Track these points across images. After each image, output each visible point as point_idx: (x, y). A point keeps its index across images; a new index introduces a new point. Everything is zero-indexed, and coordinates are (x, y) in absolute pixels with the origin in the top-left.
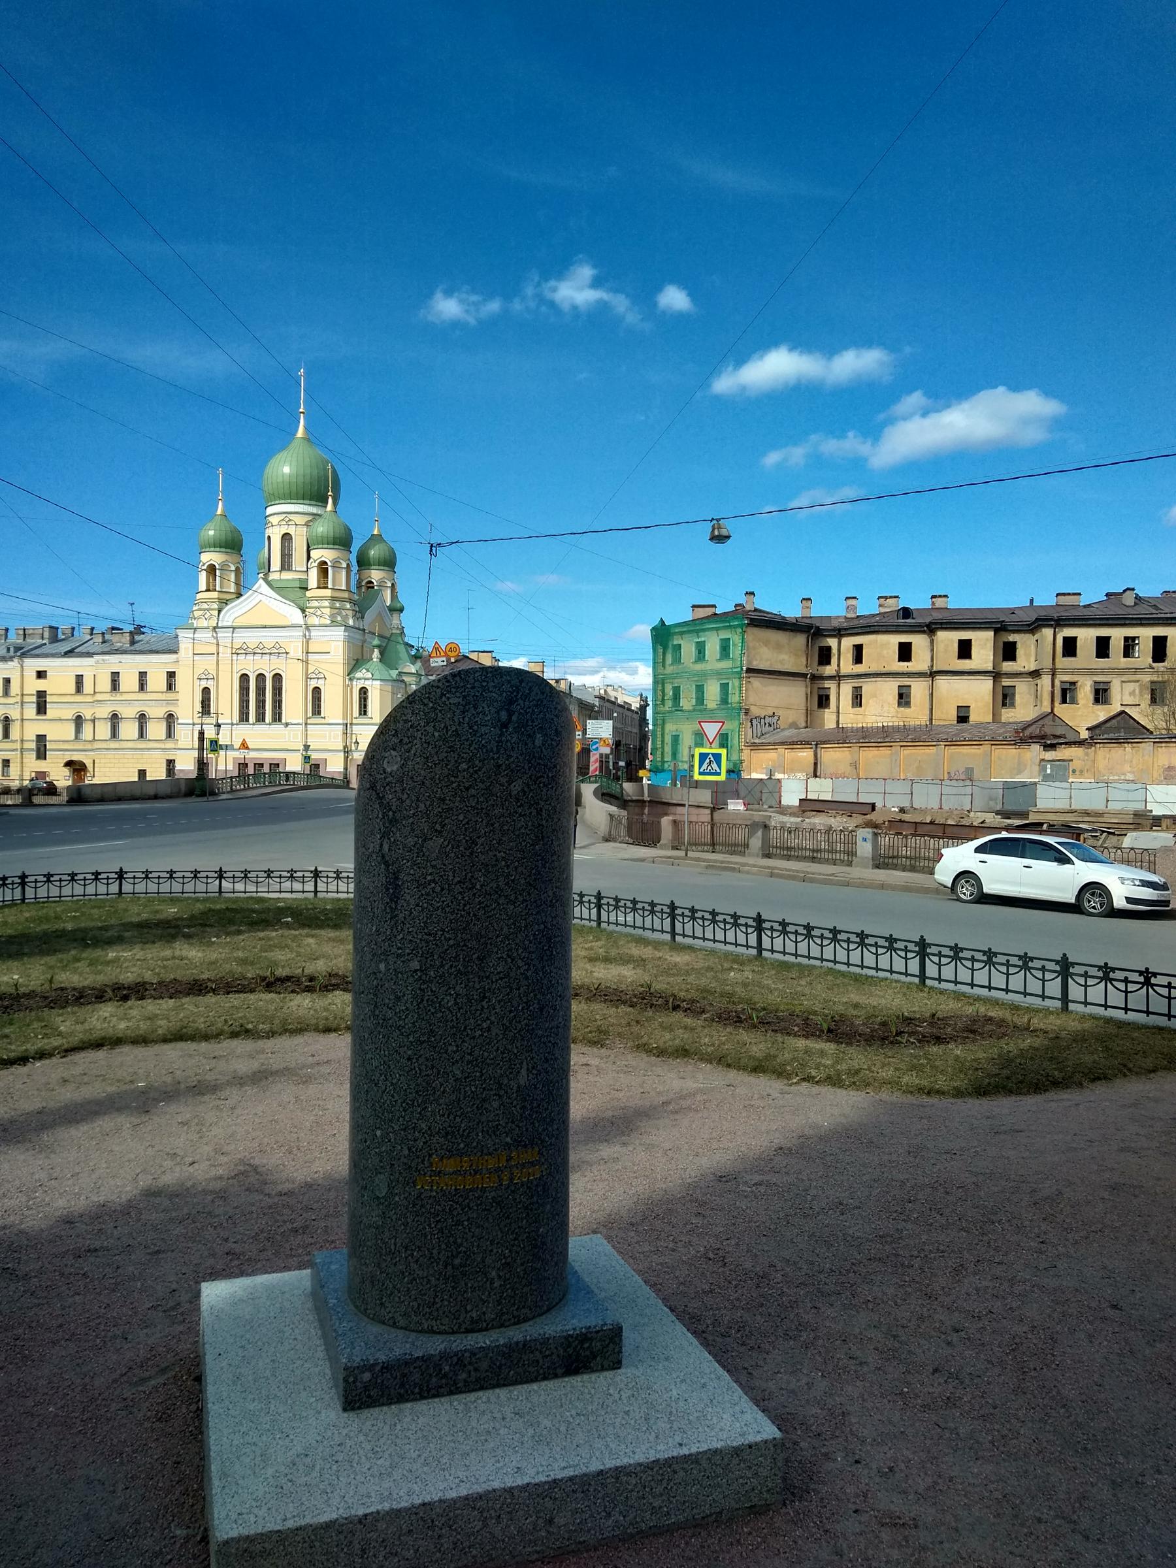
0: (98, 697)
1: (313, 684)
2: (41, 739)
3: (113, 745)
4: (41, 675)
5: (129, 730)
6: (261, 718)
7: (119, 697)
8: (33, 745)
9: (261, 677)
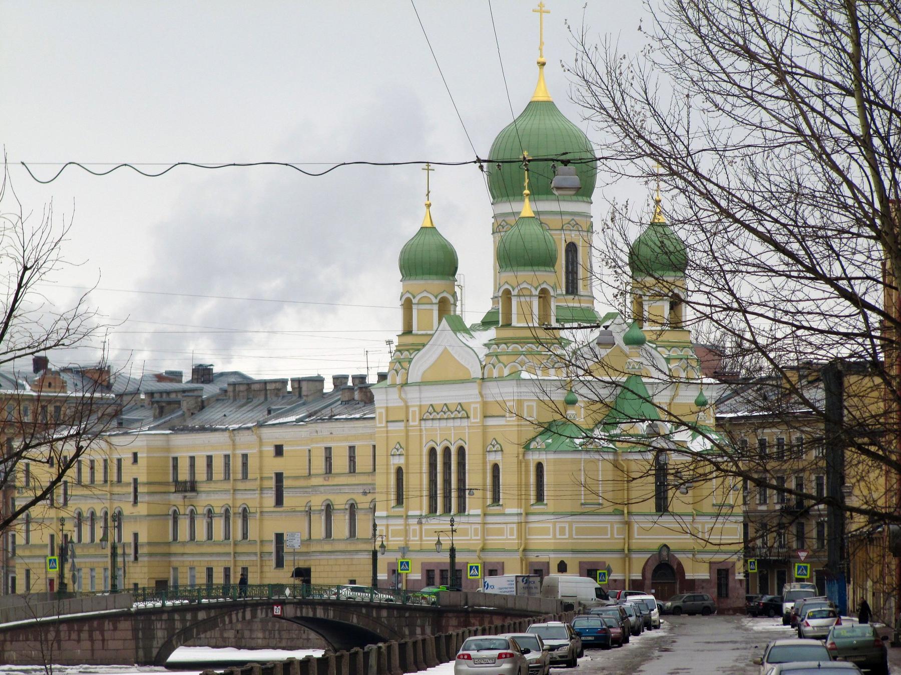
0: (315, 481)
1: (492, 458)
2: (279, 537)
4: (279, 451)
8: (272, 548)
9: (447, 451)
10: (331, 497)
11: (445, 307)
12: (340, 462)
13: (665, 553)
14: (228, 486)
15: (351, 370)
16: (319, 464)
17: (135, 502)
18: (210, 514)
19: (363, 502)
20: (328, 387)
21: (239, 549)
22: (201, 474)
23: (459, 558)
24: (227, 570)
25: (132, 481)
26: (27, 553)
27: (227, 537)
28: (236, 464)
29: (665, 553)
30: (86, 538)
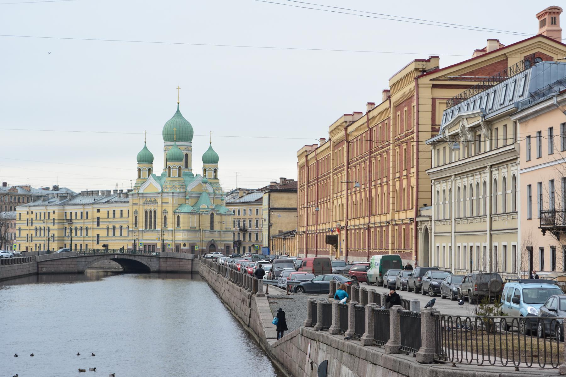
2: (98, 236)
3: (114, 239)
4: (98, 211)
5: (118, 232)
6: (151, 228)
7: (115, 220)
8: (96, 239)
9: (151, 212)
10: (115, 224)
11: (150, 170)
12: (118, 214)
13: (213, 241)
14: (82, 221)
15: (119, 189)
16: (111, 215)
17: (54, 225)
18: (76, 229)
19: (125, 226)
20: (112, 193)
21: (86, 239)
22: (74, 217)
23: (165, 242)
24: (81, 245)
25: (53, 219)
26: (20, 239)
27: (81, 235)
28: (84, 215)
29: (213, 241)
30: (38, 235)
